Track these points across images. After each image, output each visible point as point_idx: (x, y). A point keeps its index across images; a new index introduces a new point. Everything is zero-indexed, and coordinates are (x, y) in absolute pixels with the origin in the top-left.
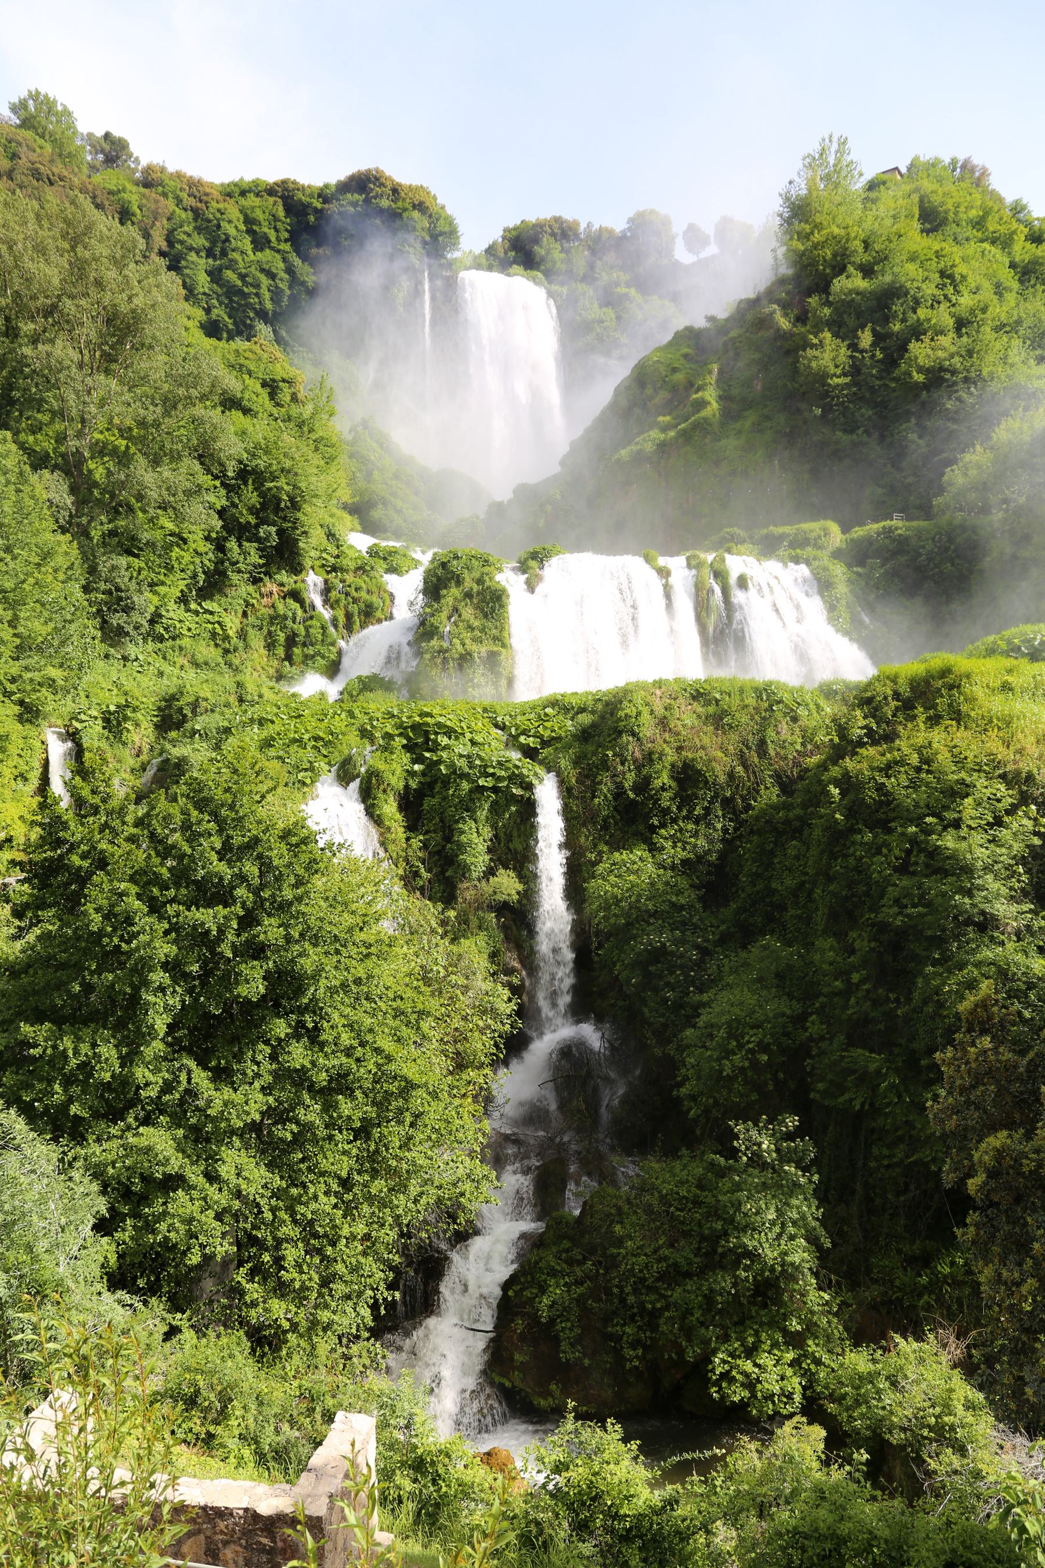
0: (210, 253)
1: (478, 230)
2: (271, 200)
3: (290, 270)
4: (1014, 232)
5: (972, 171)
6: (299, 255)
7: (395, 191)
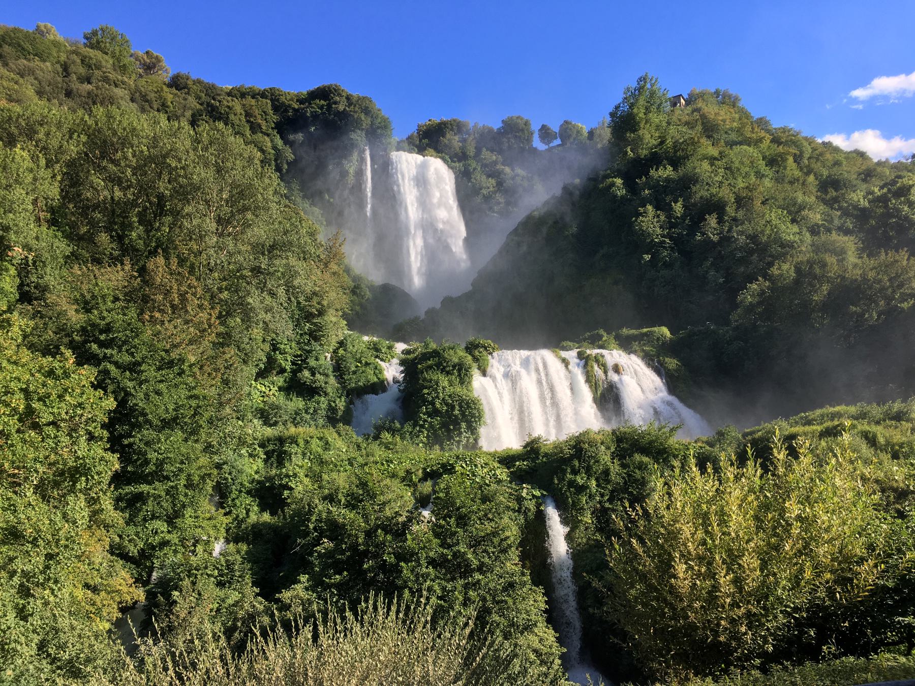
1: (404, 125)
3: (275, 148)
5: (730, 96)
6: (282, 138)
7: (348, 98)
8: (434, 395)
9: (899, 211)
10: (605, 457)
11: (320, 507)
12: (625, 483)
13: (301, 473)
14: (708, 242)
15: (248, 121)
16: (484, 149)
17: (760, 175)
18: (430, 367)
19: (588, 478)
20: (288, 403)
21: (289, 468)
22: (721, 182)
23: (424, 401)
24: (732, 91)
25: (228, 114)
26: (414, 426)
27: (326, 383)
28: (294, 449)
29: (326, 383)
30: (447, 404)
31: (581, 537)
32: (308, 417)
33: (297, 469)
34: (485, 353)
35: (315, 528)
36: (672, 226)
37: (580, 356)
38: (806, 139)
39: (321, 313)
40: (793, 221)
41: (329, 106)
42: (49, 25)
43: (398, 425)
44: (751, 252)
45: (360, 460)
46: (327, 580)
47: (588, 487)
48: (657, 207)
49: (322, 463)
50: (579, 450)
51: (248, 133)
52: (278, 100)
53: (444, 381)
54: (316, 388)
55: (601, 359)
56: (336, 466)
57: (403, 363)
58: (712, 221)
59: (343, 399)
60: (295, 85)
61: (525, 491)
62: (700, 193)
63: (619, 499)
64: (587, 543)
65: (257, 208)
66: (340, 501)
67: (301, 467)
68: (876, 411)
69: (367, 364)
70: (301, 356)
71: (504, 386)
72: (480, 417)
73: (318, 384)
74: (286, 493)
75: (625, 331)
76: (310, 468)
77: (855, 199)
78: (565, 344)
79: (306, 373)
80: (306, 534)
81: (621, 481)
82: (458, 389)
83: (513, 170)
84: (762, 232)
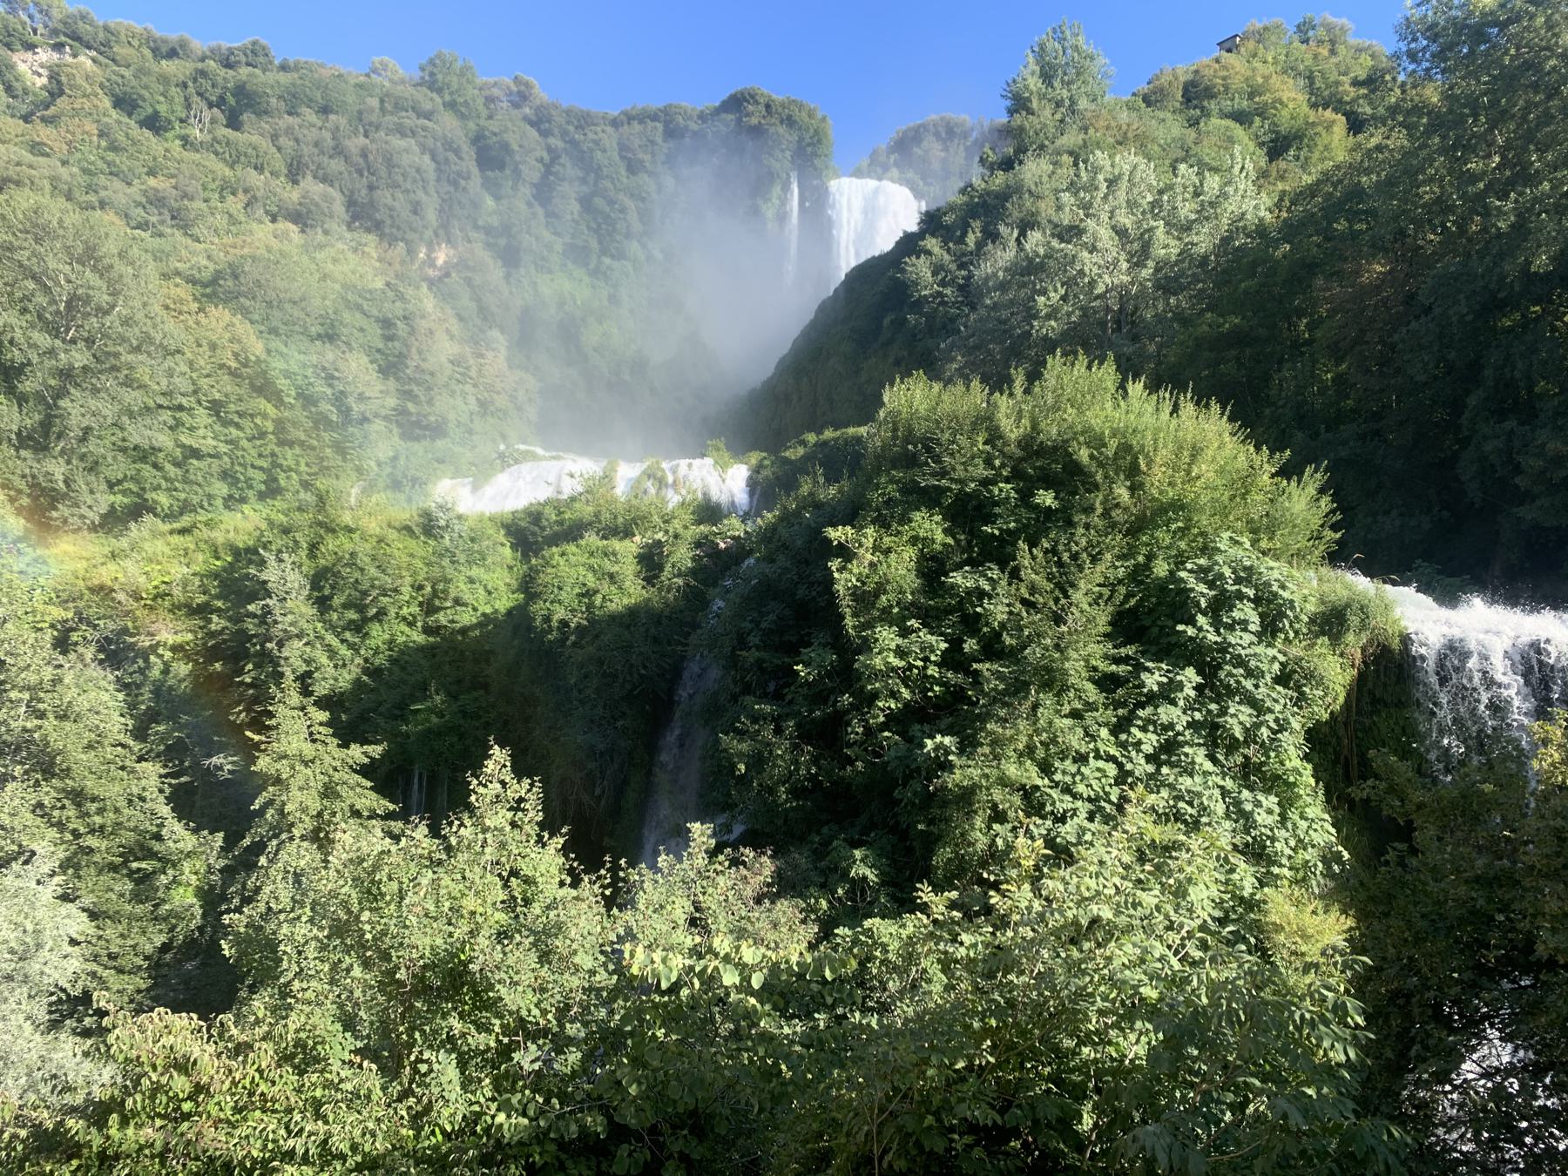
0: (584, 181)
15: (623, 158)
25: (591, 150)
42: (386, 58)
51: (623, 172)
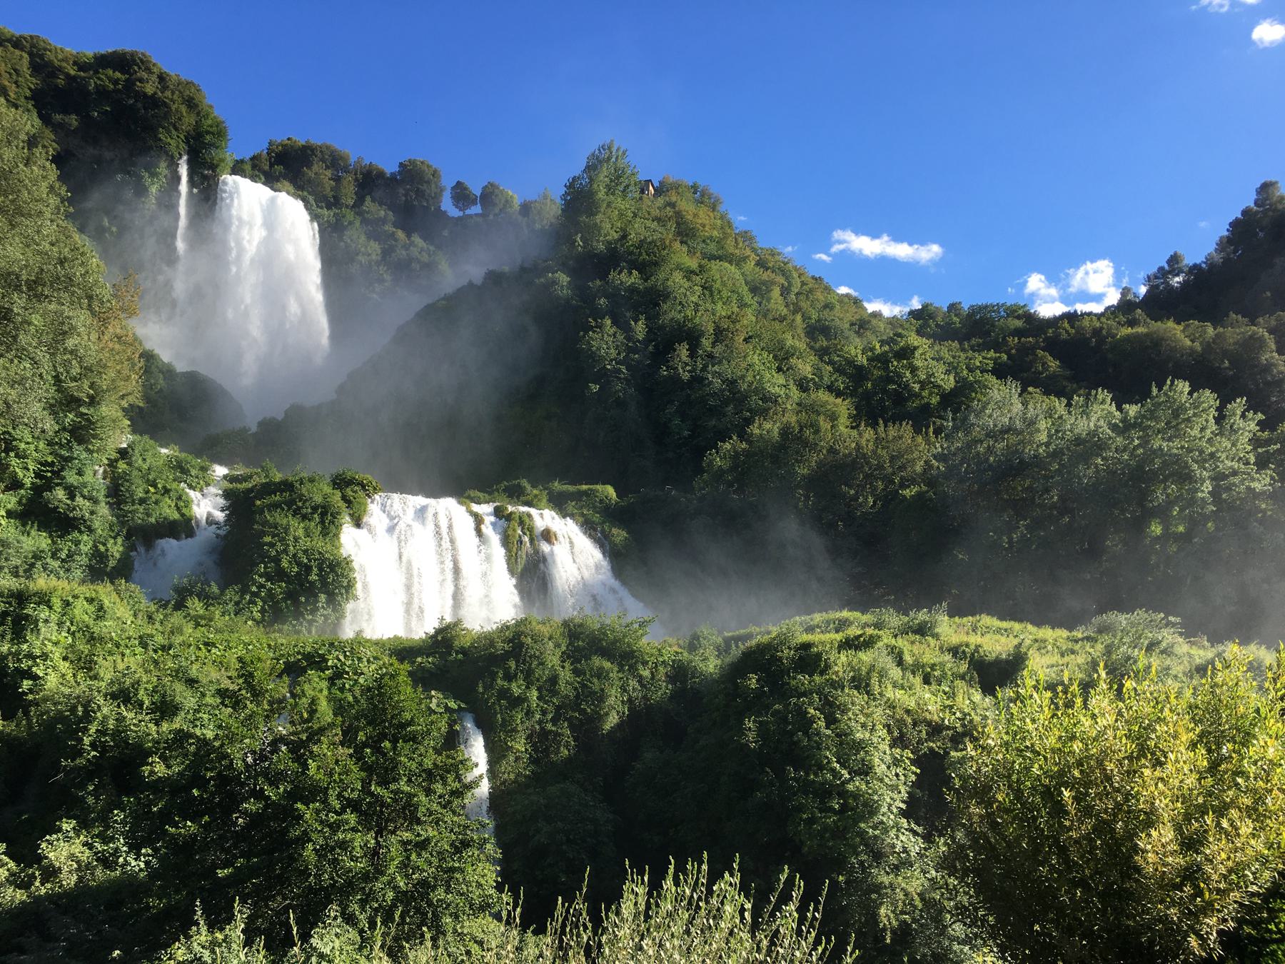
2: (18, 52)
4: (748, 257)
7: (162, 78)
8: (279, 547)
9: (900, 376)
10: (553, 660)
11: (105, 710)
12: (577, 697)
13: (57, 654)
14: (675, 379)
16: (368, 198)
17: (742, 305)
18: (276, 506)
19: (527, 687)
20: (24, 538)
21: (34, 643)
22: (697, 305)
23: (264, 557)
24: (713, 190)
26: (244, 591)
27: (92, 513)
28: (44, 613)
29: (92, 513)
30: (299, 564)
31: (509, 770)
32: (56, 564)
33: (50, 646)
34: (361, 493)
35: (93, 745)
36: (635, 350)
37: (498, 512)
38: (796, 269)
39: (93, 401)
40: (779, 370)
41: (130, 84)
43: (215, 589)
44: (726, 402)
45: (160, 639)
46: (172, 830)
47: (526, 699)
48: (614, 323)
49: (92, 639)
50: (512, 648)
52: (42, 57)
53: (297, 528)
54: (75, 519)
55: (527, 520)
56: (118, 645)
57: (227, 494)
58: (683, 351)
59: (120, 540)
60: (75, 40)
61: (434, 700)
62: (670, 314)
63: (566, 719)
64: (515, 782)
65: (19, 212)
66: (141, 704)
67: (56, 644)
68: (894, 619)
69: (167, 491)
70: (52, 464)
71: (388, 545)
72: (350, 586)
73: (77, 513)
74: (26, 684)
75: (557, 486)
76: (71, 646)
77: (853, 352)
78: (472, 493)
79: (60, 493)
80: (79, 753)
81: (572, 694)
82: (319, 544)
83: (409, 236)
84: (743, 377)
